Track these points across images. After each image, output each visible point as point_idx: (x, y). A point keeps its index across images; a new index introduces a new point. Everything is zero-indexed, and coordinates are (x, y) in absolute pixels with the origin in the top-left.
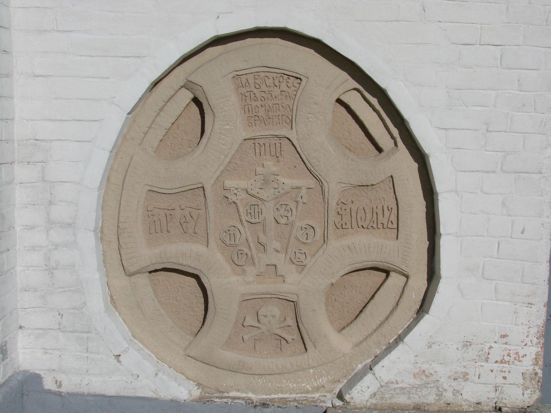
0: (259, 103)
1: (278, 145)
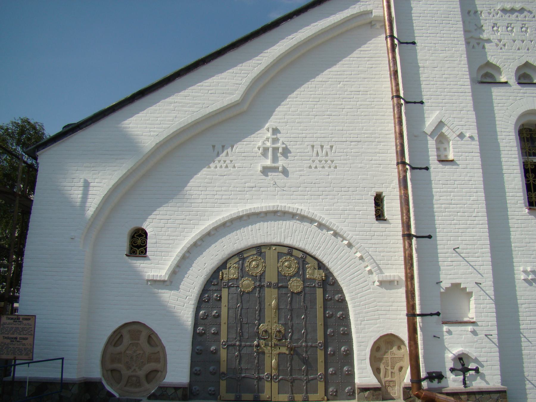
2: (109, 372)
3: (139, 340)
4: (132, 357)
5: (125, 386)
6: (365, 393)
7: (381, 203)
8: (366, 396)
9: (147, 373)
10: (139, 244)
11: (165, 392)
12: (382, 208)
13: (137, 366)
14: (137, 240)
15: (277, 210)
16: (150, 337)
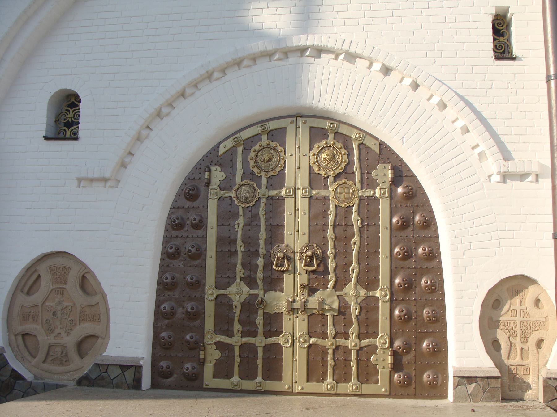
0: (58, 277)
1: (63, 291)
2: (20, 338)
3: (66, 283)
4: (54, 312)
5: (44, 362)
6: (468, 387)
7: (507, 30)
8: (469, 393)
9: (79, 339)
10: (70, 120)
11: (106, 373)
12: (509, 39)
13: (63, 328)
14: (68, 113)
15: (305, 44)
16: (84, 277)
